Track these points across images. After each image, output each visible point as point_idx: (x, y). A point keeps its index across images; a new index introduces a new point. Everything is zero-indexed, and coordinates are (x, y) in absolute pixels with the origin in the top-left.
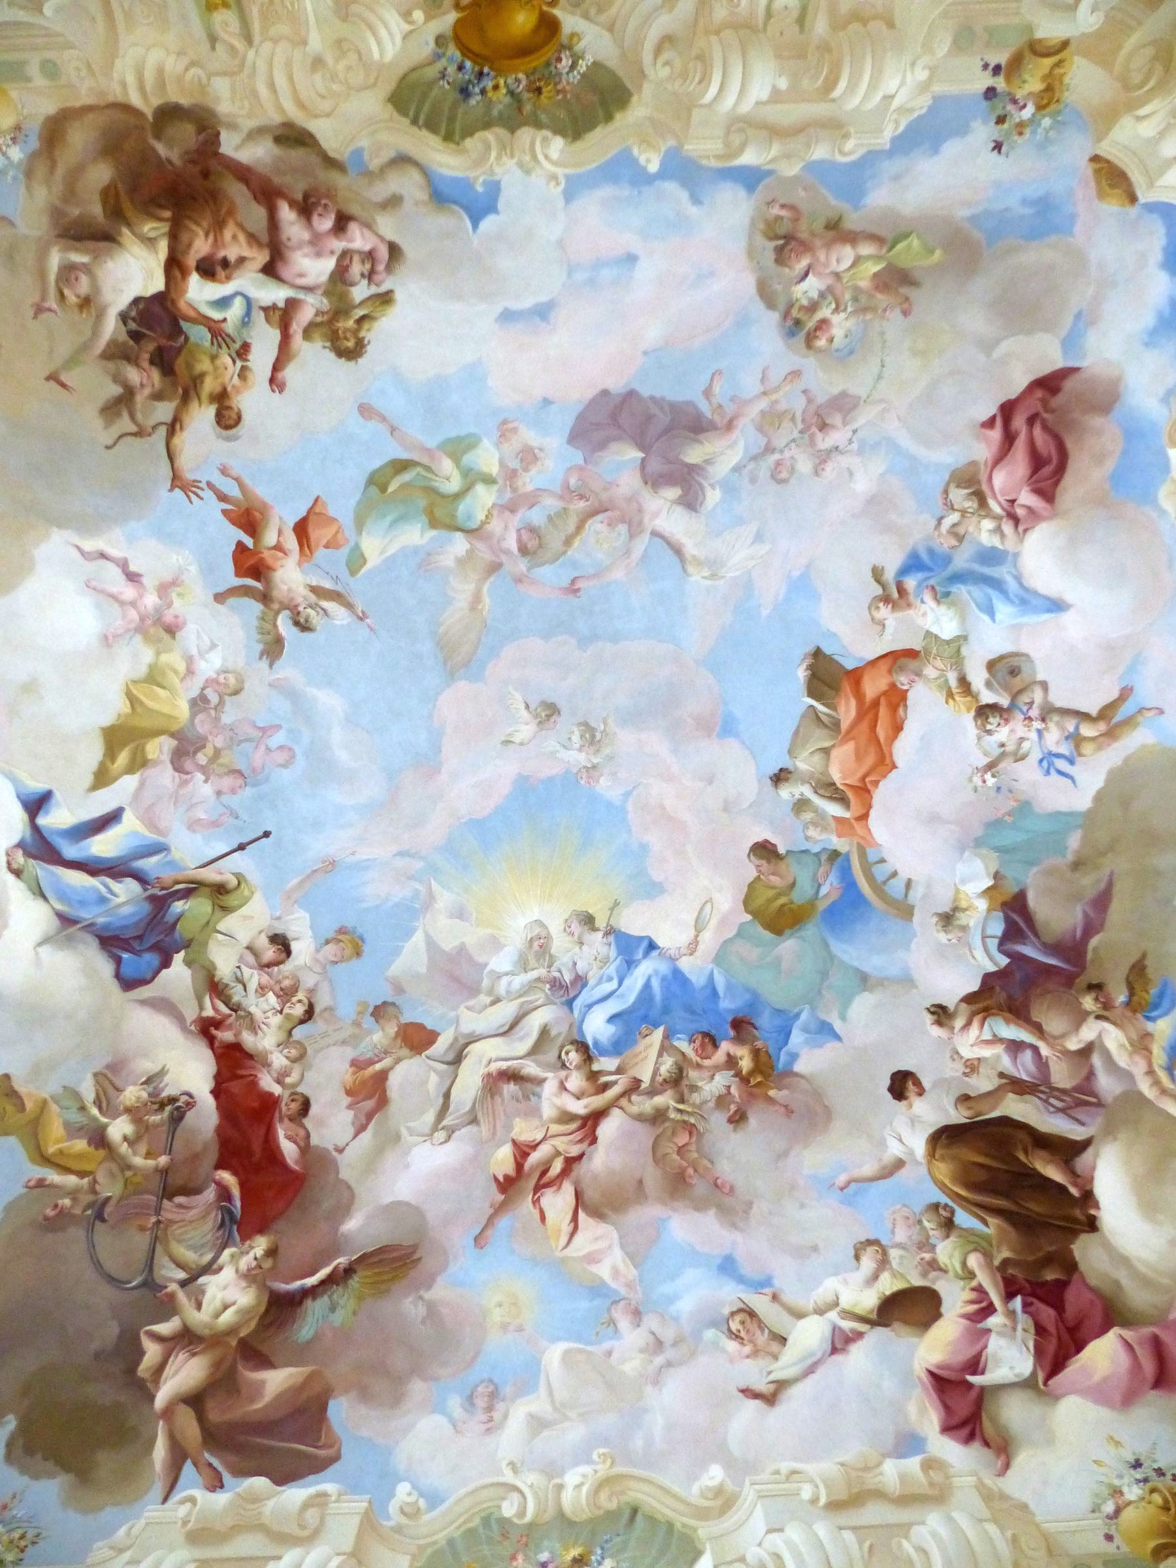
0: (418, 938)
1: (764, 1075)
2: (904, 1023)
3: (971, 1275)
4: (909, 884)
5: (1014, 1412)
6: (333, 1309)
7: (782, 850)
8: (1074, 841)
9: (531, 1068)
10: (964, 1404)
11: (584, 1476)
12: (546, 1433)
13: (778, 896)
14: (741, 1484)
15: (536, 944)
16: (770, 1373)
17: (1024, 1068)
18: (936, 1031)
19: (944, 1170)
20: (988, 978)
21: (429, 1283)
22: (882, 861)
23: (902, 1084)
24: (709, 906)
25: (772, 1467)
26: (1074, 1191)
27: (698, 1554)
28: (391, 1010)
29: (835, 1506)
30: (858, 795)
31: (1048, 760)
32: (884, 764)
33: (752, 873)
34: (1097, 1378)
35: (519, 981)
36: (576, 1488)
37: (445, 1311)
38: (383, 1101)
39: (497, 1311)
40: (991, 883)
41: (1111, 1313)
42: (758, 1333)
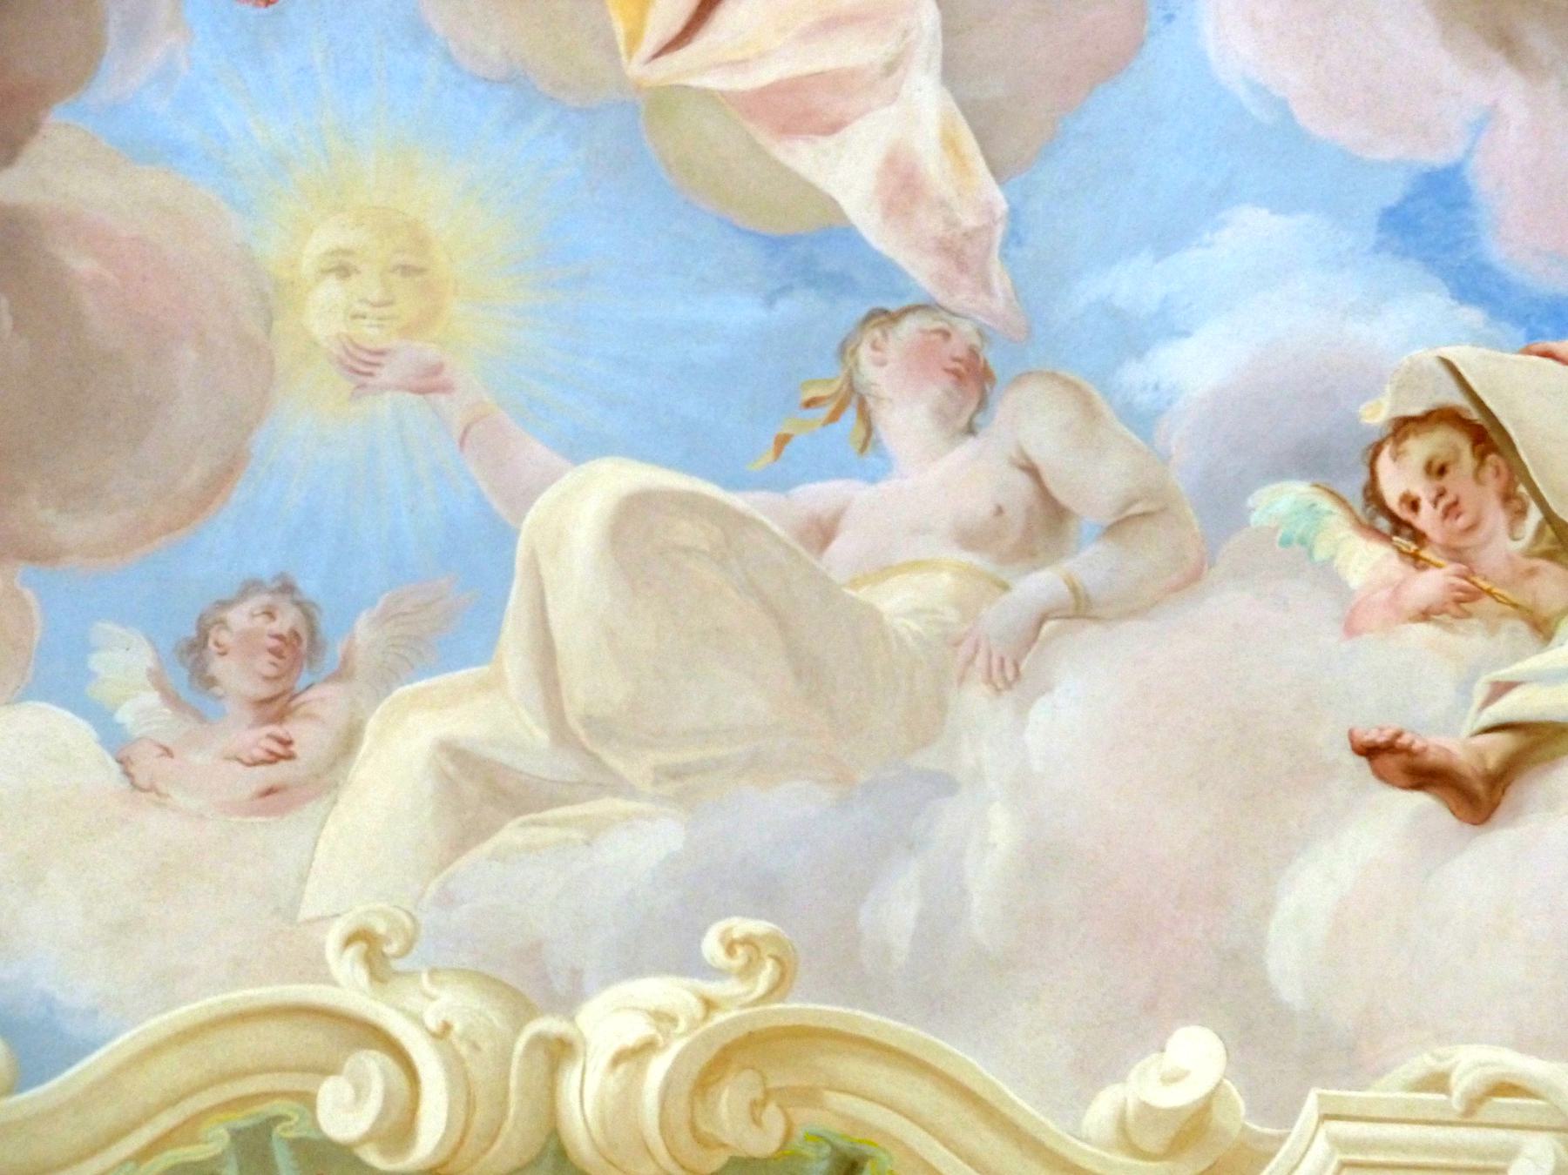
11: (663, 1018)
12: (512, 833)
14: (1288, 1116)
16: (1501, 689)
25: (1422, 1063)
37: (83, 265)
39: (330, 291)
42: (1496, 518)
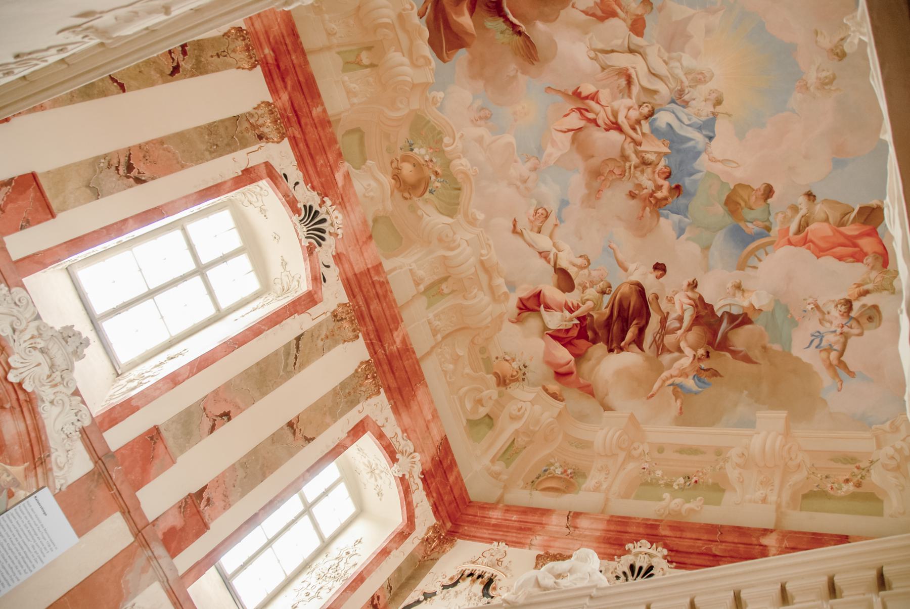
0: (690, 11)
1: (657, 204)
2: (690, 266)
3: (584, 303)
4: (755, 267)
5: (533, 323)
6: (502, 32)
7: (769, 201)
8: (776, 347)
9: (635, 89)
10: (532, 305)
13: (745, 202)
15: (700, 76)
17: (672, 323)
18: (685, 283)
19: (626, 289)
20: (711, 307)
21: (524, 72)
22: (767, 254)
23: (660, 268)
24: (735, 165)
26: (623, 344)
27: (452, 217)
28: (649, 8)
29: (482, 263)
30: (802, 237)
31: (820, 336)
32: (820, 252)
33: (756, 186)
34: (553, 352)
35: (680, 73)
36: (461, 164)
38: (602, 19)
40: (757, 308)
41: (579, 357)
